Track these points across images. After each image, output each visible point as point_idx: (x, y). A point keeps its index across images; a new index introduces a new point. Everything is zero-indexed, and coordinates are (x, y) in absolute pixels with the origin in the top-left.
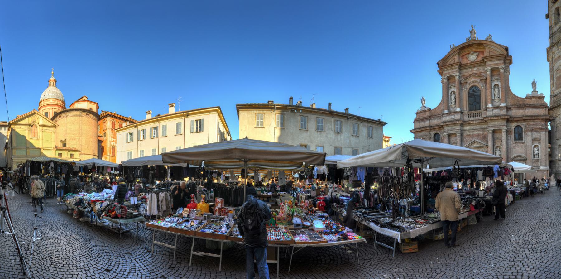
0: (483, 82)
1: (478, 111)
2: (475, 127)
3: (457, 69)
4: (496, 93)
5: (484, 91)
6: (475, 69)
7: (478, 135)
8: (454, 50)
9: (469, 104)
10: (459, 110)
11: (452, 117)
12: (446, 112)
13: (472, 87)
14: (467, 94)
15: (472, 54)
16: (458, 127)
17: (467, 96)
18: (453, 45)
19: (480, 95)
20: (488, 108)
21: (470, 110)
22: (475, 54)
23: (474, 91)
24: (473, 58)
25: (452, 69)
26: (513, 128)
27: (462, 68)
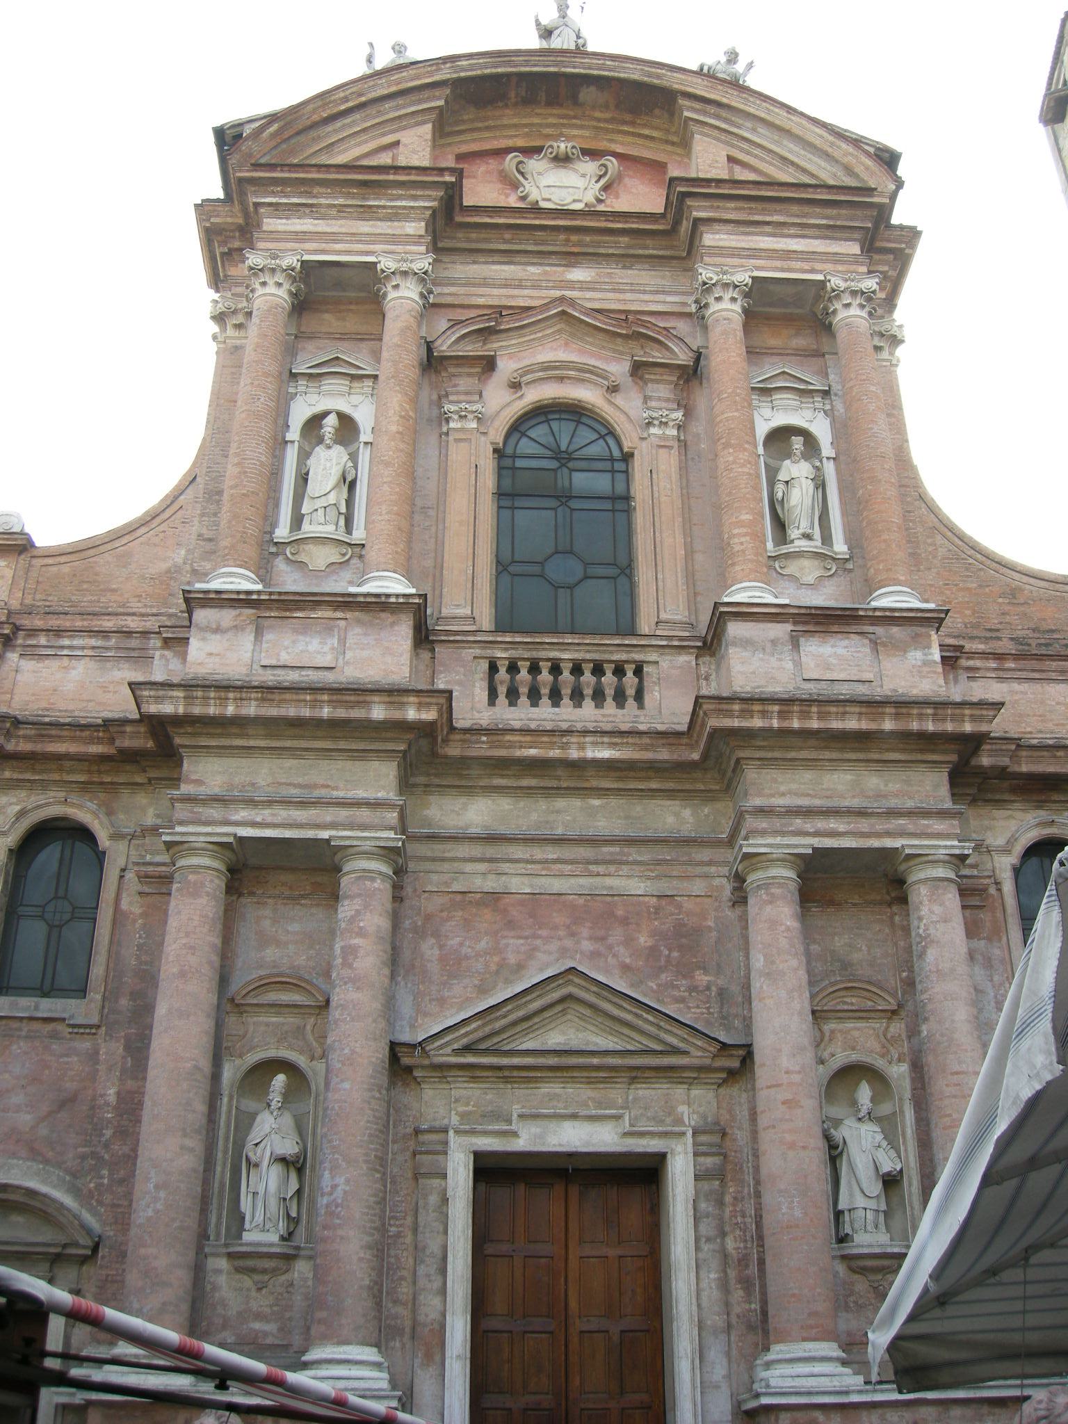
0: (661, 390)
1: (613, 650)
2: (568, 814)
3: (415, 228)
4: (800, 498)
5: (668, 463)
6: (579, 274)
7: (603, 914)
8: (409, 80)
9: (502, 566)
10: (395, 585)
11: (304, 650)
12: (240, 580)
13: (542, 412)
14: (488, 464)
15: (562, 160)
16: (378, 779)
17: (489, 481)
18: (399, 48)
19: (621, 502)
20: (745, 613)
21: (502, 625)
22: (590, 167)
23: (564, 458)
24: (564, 185)
25: (367, 213)
26: (1004, 865)
27: (460, 240)
